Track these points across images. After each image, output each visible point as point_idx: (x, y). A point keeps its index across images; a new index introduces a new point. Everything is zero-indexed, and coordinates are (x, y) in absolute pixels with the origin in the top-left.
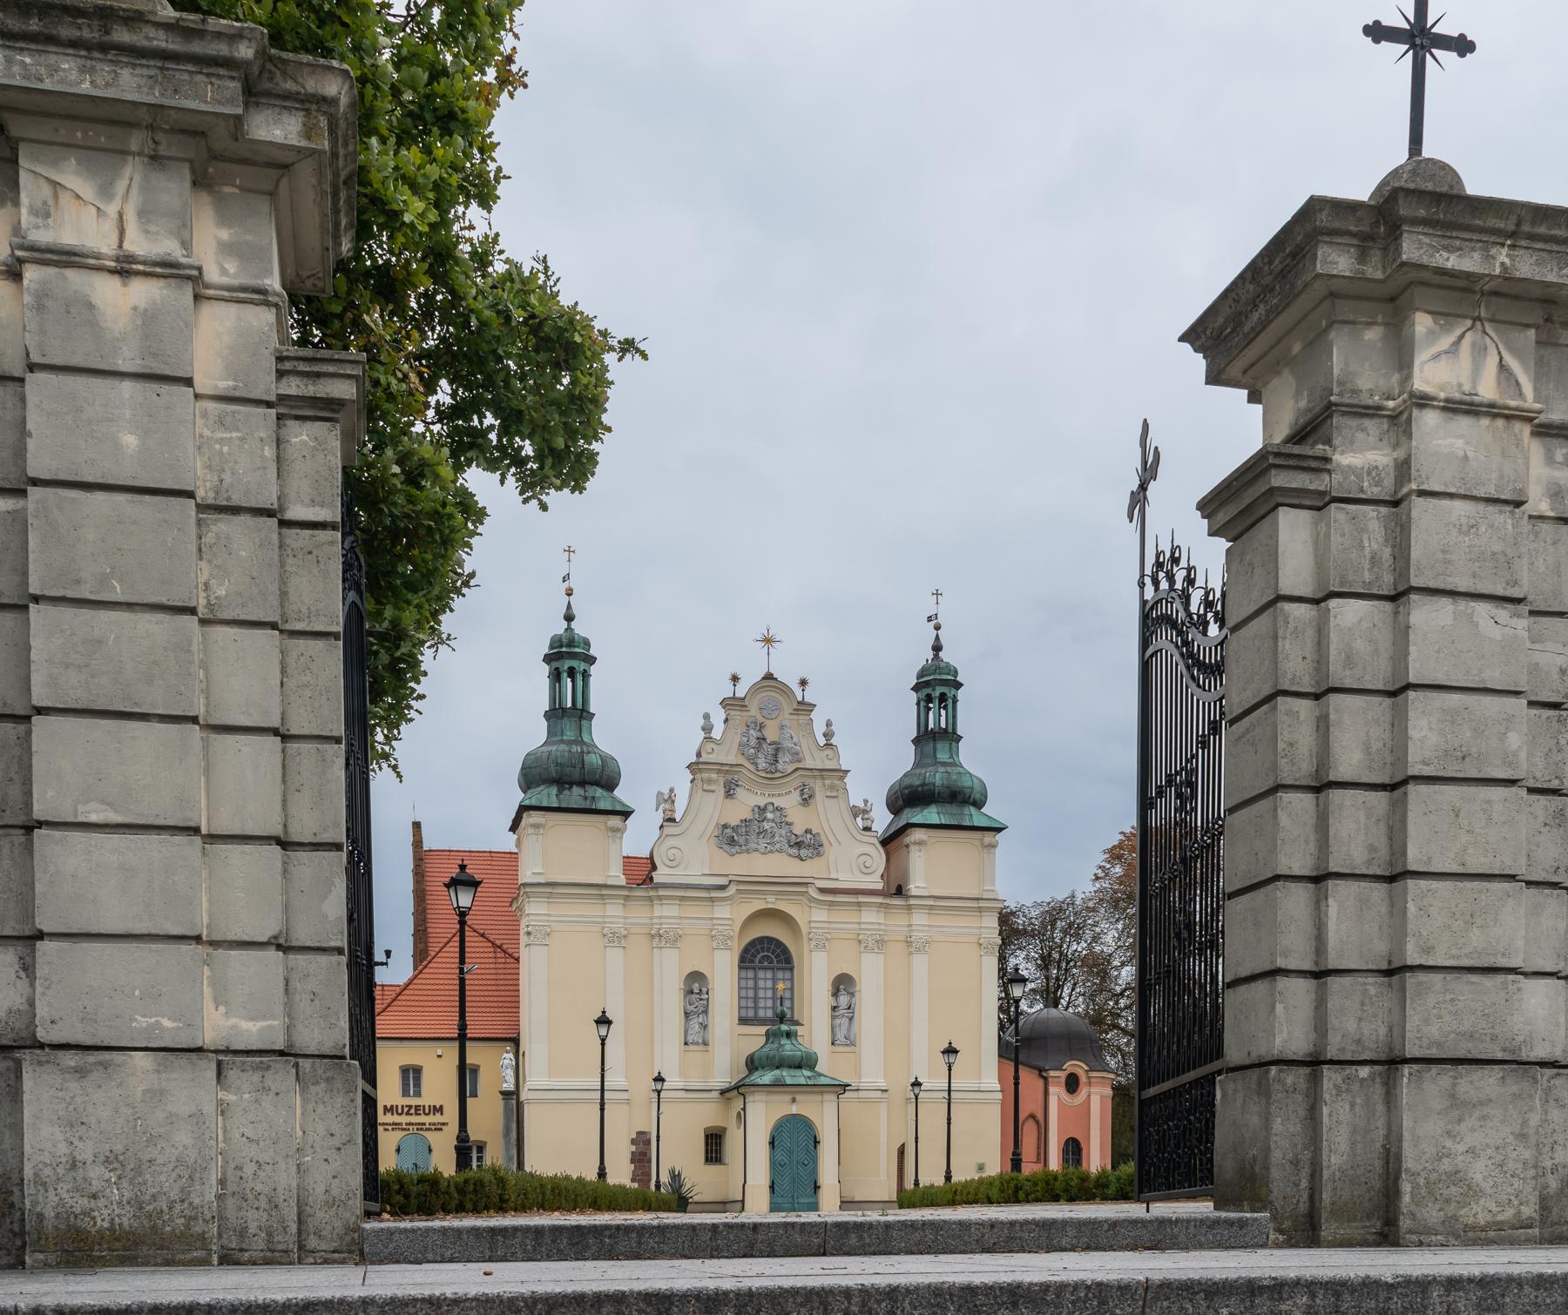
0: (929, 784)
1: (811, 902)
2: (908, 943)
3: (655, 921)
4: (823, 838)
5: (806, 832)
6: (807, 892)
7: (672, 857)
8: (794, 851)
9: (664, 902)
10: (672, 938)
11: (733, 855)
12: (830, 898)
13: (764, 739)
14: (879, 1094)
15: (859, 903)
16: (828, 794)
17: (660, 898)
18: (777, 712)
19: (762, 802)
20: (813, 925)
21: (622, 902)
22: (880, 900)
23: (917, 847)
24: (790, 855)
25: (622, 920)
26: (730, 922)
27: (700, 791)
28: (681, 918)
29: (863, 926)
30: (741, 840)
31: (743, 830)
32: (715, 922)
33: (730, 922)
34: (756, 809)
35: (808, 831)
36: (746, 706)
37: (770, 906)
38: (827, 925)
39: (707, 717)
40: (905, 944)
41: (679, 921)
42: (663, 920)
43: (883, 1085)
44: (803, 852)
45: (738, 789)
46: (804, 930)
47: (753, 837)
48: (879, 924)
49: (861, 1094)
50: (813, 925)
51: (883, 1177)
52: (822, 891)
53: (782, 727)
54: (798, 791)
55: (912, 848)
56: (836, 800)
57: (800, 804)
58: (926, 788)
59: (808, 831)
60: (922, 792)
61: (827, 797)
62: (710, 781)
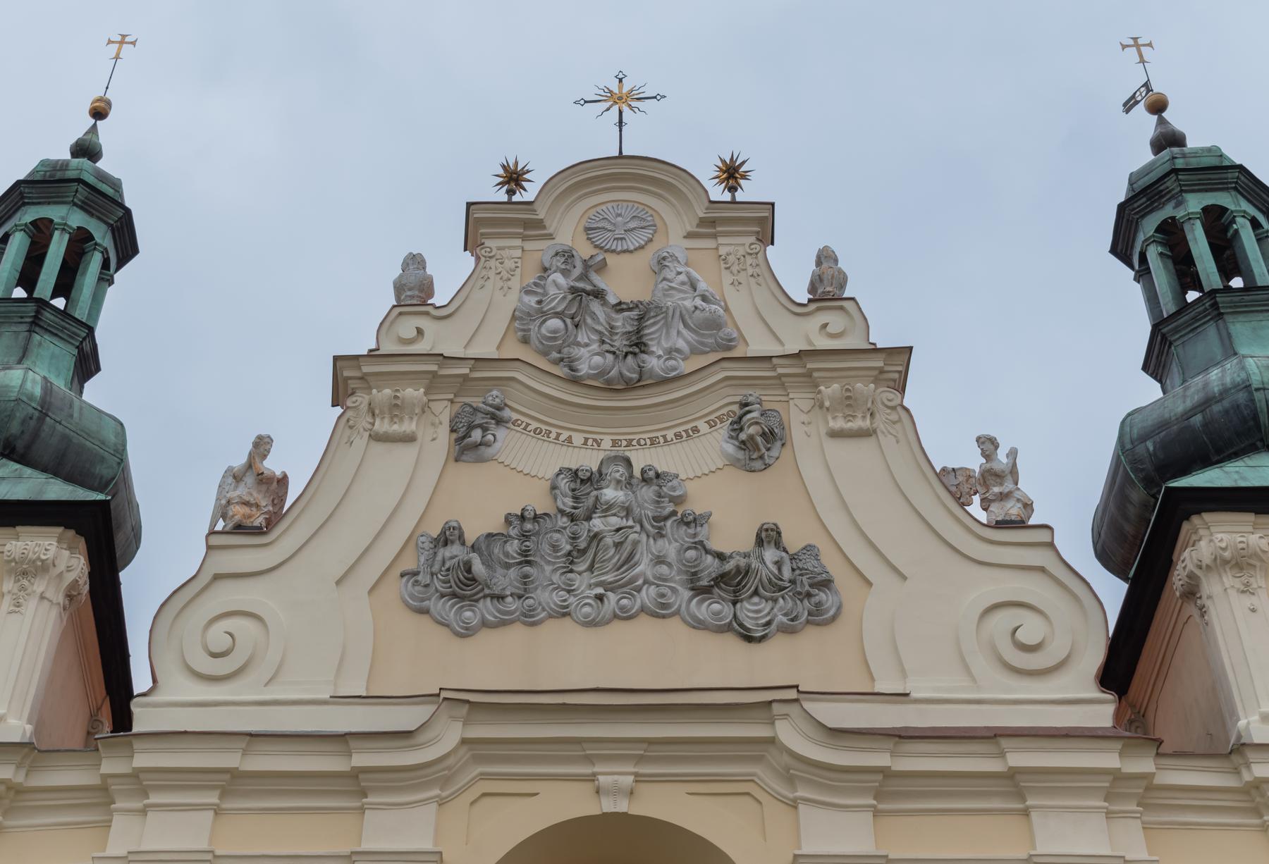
0: (1225, 392)
1: (790, 780)
4: (833, 565)
5: (760, 542)
8: (716, 608)
11: (466, 632)
12: (880, 759)
13: (599, 294)
15: (1012, 775)
16: (839, 424)
18: (645, 235)
19: (589, 460)
22: (1108, 759)
24: (698, 625)
27: (361, 442)
30: (506, 580)
31: (513, 547)
34: (564, 484)
35: (768, 536)
36: (539, 224)
39: (415, 262)
44: (752, 611)
45: (501, 433)
47: (547, 571)
53: (661, 262)
54: (723, 430)
55: (1211, 587)
56: (866, 445)
57: (734, 463)
58: (1217, 408)
59: (768, 536)
60: (1205, 425)
61: (835, 434)
62: (396, 409)
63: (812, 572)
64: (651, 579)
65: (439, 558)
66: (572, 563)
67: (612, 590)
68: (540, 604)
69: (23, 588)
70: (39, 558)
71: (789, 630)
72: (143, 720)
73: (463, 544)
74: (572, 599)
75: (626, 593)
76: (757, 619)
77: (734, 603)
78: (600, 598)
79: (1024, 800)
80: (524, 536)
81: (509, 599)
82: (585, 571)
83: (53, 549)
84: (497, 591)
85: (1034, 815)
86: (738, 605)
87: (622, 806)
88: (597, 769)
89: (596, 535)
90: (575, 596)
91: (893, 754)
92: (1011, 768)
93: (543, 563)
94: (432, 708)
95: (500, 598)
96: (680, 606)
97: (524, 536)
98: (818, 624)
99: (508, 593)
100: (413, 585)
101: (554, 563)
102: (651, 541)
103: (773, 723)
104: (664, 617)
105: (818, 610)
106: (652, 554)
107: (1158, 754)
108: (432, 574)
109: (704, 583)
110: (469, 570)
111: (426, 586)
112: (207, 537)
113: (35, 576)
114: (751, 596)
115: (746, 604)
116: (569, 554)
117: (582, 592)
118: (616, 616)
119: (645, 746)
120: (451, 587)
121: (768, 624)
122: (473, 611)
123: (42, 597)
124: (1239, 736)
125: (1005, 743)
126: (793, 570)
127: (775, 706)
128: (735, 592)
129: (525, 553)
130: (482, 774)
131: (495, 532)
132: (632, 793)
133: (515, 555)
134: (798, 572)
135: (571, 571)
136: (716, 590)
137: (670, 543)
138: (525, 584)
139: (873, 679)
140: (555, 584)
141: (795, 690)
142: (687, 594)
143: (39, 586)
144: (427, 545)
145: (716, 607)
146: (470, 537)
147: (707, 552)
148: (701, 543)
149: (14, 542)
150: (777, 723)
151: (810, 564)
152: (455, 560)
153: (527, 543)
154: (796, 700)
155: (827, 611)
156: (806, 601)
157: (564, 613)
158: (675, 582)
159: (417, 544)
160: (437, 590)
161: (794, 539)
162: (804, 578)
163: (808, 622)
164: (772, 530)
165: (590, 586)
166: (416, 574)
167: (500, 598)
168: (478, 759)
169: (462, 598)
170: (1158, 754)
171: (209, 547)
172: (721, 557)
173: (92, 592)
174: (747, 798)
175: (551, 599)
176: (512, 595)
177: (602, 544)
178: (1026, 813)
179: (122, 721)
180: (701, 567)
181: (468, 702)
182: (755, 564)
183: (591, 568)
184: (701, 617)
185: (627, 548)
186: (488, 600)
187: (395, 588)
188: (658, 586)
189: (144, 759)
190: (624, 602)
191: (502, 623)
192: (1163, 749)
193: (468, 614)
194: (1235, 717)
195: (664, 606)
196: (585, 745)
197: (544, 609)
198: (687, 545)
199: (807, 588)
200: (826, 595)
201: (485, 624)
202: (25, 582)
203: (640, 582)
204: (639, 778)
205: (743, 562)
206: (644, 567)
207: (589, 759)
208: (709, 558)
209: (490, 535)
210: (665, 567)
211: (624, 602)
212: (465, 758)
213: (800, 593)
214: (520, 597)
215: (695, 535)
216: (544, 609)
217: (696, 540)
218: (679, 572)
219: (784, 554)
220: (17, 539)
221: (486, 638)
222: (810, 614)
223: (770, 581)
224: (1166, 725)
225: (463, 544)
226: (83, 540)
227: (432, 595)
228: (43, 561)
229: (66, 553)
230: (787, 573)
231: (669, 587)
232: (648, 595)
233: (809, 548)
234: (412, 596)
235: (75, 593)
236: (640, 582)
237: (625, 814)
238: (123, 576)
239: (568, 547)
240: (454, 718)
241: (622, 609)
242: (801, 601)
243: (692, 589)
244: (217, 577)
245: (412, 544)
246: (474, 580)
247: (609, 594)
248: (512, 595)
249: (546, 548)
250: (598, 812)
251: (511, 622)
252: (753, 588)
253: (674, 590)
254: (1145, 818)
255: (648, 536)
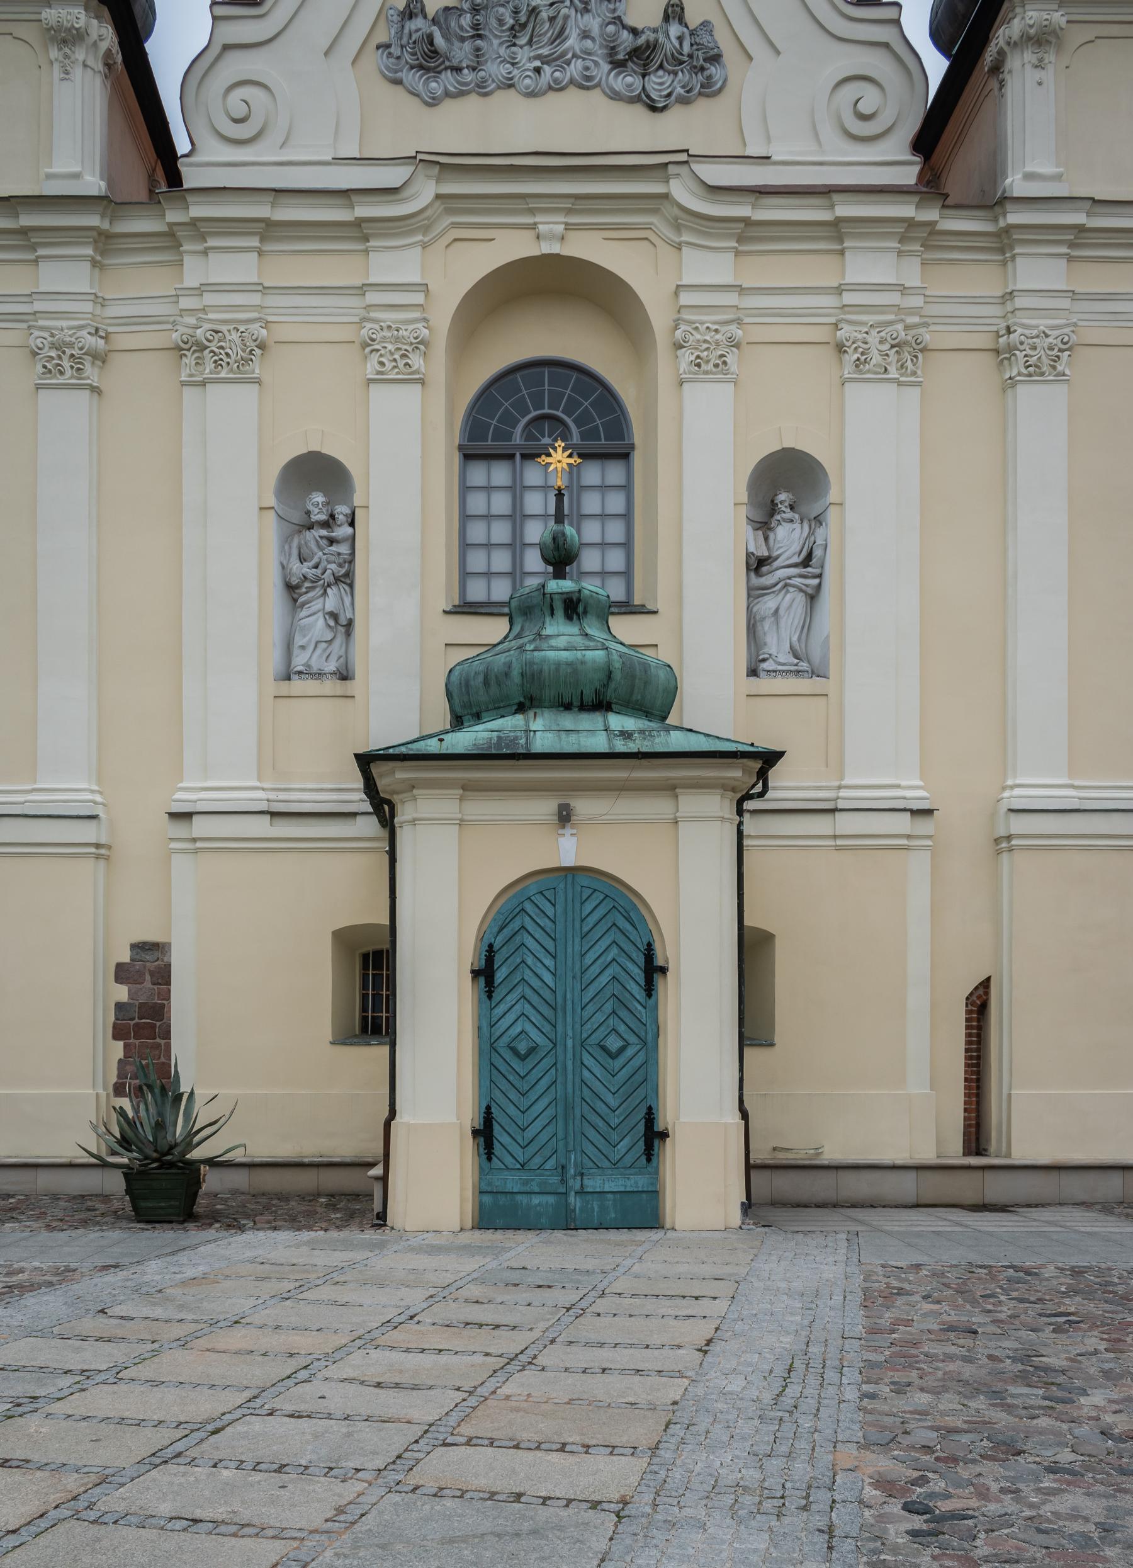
1: (678, 228)
2: (1002, 354)
3: (185, 303)
4: (723, 40)
5: (667, 18)
6: (666, 196)
7: (240, 111)
9: (212, 242)
10: (236, 353)
11: (433, 102)
14: (902, 824)
17: (199, 229)
20: (686, 299)
21: (89, 251)
22: (906, 210)
23: (1029, 56)
24: (615, 96)
25: (88, 307)
26: (419, 298)
28: (265, 290)
29: (848, 298)
30: (461, 53)
31: (466, 20)
32: (372, 298)
33: (419, 298)
37: (547, 248)
38: (731, 299)
40: (988, 359)
41: (255, 299)
42: (209, 299)
43: (917, 794)
44: (658, 83)
46: (659, 317)
47: (494, 46)
48: (903, 289)
49: (846, 824)
50: (686, 299)
51: (917, 1086)
52: (716, 191)
63: (706, 47)
64: (579, 53)
65: (406, 31)
66: (515, 37)
67: (548, 63)
68: (490, 76)
69: (66, 56)
70: (73, 26)
71: (684, 101)
72: (191, 178)
73: (425, 17)
74: (516, 72)
75: (558, 66)
76: (660, 90)
77: (644, 76)
78: (538, 70)
79: (841, 241)
80: (475, 10)
81: (466, 71)
82: (525, 45)
83: (83, 16)
84: (455, 63)
85: (847, 254)
86: (647, 78)
87: (555, 248)
88: (537, 219)
89: (534, 9)
90: (518, 68)
91: (754, 207)
92: (837, 218)
93: (491, 37)
94: (411, 169)
95: (458, 70)
96: (601, 78)
97: (475, 10)
98: (708, 96)
99: (465, 65)
100: (388, 57)
101: (500, 37)
102: (579, 15)
103: (668, 182)
104: (588, 88)
105: (708, 83)
106: (580, 28)
107: (943, 206)
108: (402, 47)
109: (621, 57)
110: (431, 43)
111: (398, 58)
112: (211, 7)
113: (74, 44)
114: (657, 70)
115: (653, 77)
116: (512, 28)
117: (524, 65)
118: (550, 88)
119: (572, 200)
120: (418, 59)
121: (669, 95)
122: (437, 82)
123: (85, 66)
124: (1004, 191)
125: (836, 197)
126: (692, 45)
127: (670, 167)
128: (645, 65)
129: (476, 26)
130: (452, 223)
131: (451, 5)
132: (563, 238)
133: (468, 29)
134: (695, 47)
135: (514, 45)
136: (630, 64)
137: (594, 18)
138: (477, 56)
139: (745, 145)
140: (500, 57)
141: (686, 154)
142: (606, 67)
143: (80, 54)
144: (396, 18)
145: (629, 79)
146: (431, 10)
147: (624, 27)
148: (619, 18)
149: (48, 10)
150: (671, 181)
151: (705, 39)
152: (420, 33)
153: (478, 17)
154: (686, 162)
155: (716, 83)
156: (699, 74)
157: (509, 84)
158: (597, 56)
159: (387, 17)
160: (407, 62)
161: (693, 17)
162: (700, 53)
163: (700, 94)
164: (677, 5)
165: (530, 60)
166: (388, 46)
167: (458, 70)
168: (449, 211)
169: (428, 70)
170: (943, 206)
171: (214, 18)
172: (635, 32)
173: (125, 60)
174: (646, 243)
175: (500, 72)
176: (468, 67)
177: (539, 18)
178: (842, 252)
179: (174, 179)
180: (618, 42)
181: (438, 163)
182: (662, 39)
183: (530, 43)
184: (617, 89)
185: (559, 22)
186: (449, 71)
187: (373, 60)
188: (584, 59)
189: (198, 210)
190: (557, 74)
191: (461, 94)
192: (949, 201)
193: (434, 85)
194: (1005, 176)
195: (588, 78)
196: (528, 200)
197: (493, 81)
198: (607, 20)
199: (701, 62)
200: (716, 68)
201: (448, 94)
202: (67, 50)
203: (569, 56)
204: (569, 227)
205: (652, 37)
206: (572, 42)
207: (532, 212)
208: (625, 33)
209: (447, 9)
210: (589, 41)
211: (557, 74)
212: (439, 212)
213: (695, 67)
214: (474, 69)
215: (614, 10)
216: (493, 81)
217: (616, 15)
218: (601, 46)
219: (685, 30)
220: (50, 7)
221: (449, 106)
222: (702, 86)
223: (673, 55)
224: (955, 183)
225: (425, 17)
226: (106, 9)
227: (404, 67)
228: (77, 29)
229: (95, 22)
230: (686, 49)
231: (593, 60)
232: (575, 69)
233: (705, 24)
234: (388, 68)
235: (111, 62)
236: (569, 56)
237: (558, 255)
238: (146, 45)
239: (511, 22)
240: (428, 177)
241: (556, 81)
242: (696, 74)
243: (611, 63)
244: (226, 48)
245: (383, 16)
246: (436, 52)
247: (545, 66)
248: (468, 67)
249: (493, 22)
250: (539, 254)
251: (468, 93)
252: (659, 62)
253: (596, 63)
254: (924, 256)
255: (576, 11)
